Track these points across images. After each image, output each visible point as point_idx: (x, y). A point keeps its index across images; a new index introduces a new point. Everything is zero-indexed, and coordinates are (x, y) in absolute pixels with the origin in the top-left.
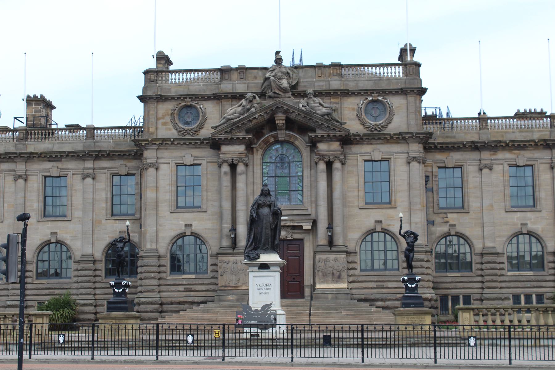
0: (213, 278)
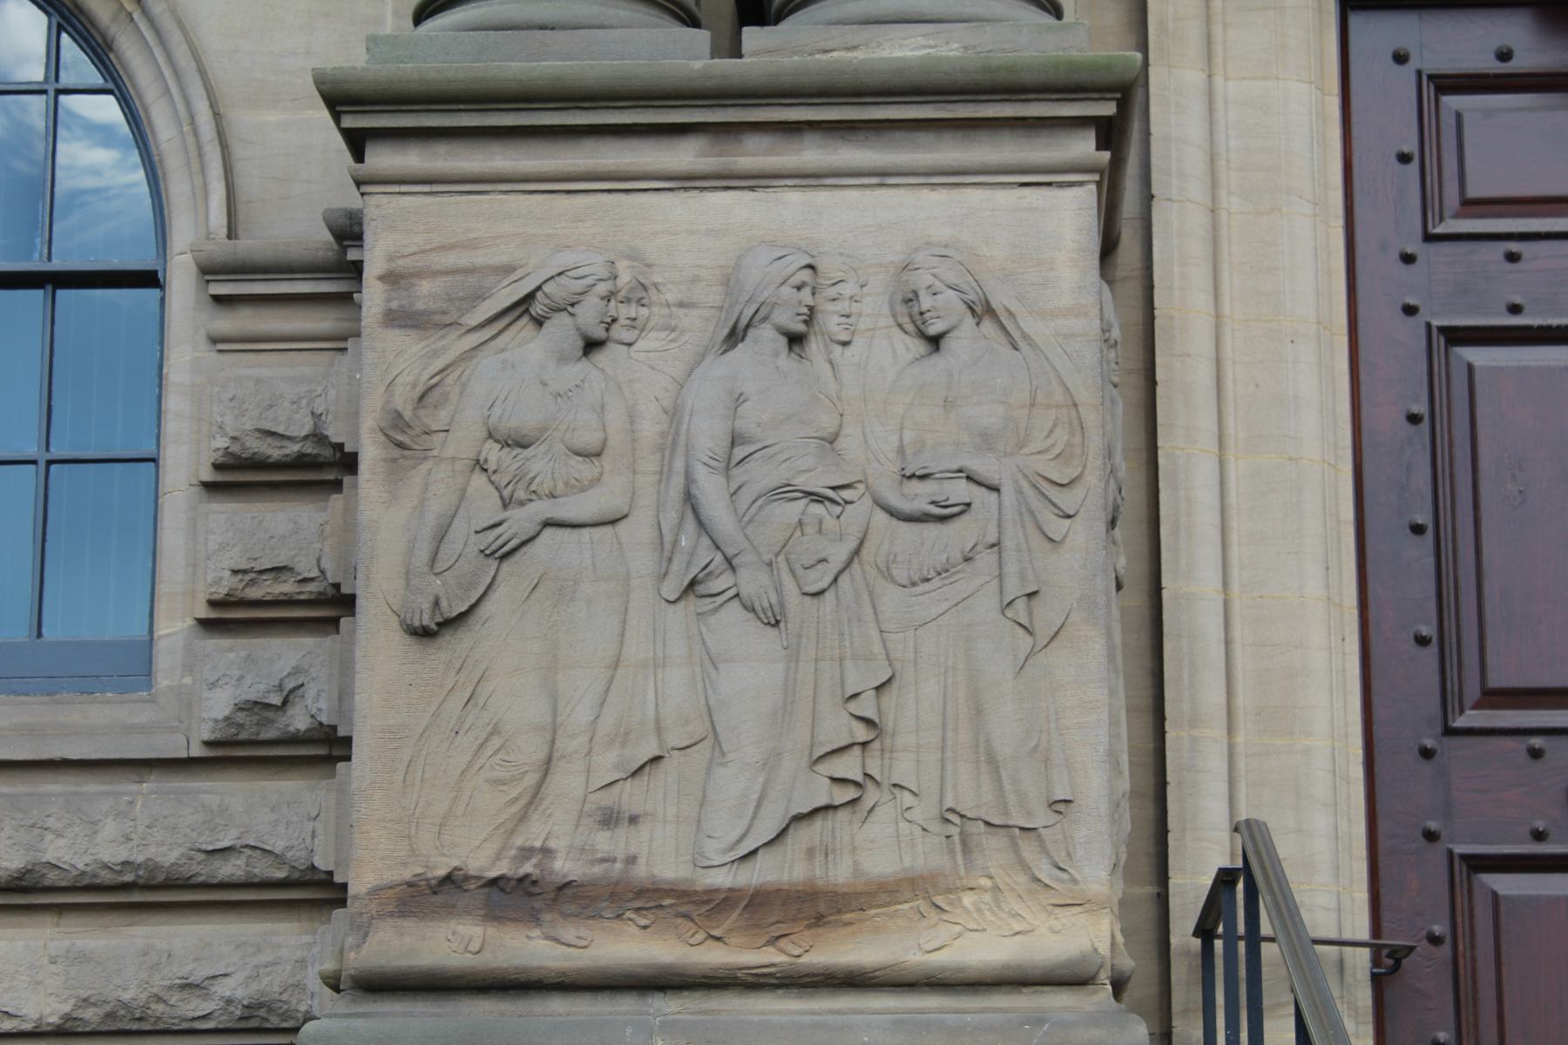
0: (232, 753)
